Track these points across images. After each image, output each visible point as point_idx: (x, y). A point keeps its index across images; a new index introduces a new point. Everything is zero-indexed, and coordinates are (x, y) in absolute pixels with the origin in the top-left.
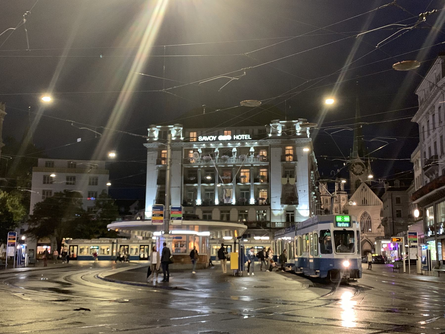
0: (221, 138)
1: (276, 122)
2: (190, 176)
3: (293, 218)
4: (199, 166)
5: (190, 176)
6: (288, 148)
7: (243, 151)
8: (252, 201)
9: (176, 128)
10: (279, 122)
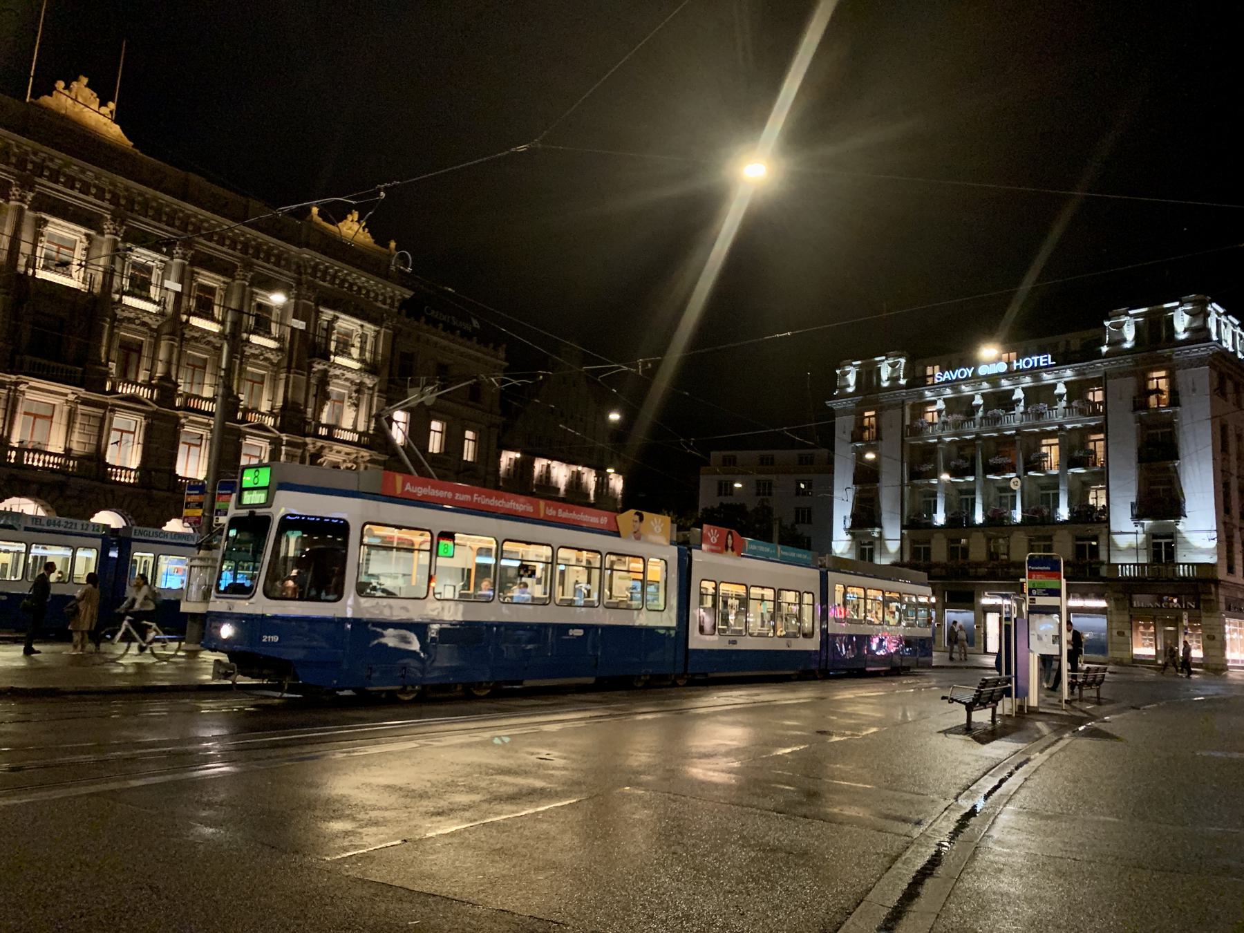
1: (1119, 315)
2: (926, 461)
3: (1171, 553)
4: (939, 438)
5: (920, 461)
6: (1156, 374)
7: (1040, 395)
8: (1063, 513)
9: (891, 361)
10: (1127, 314)
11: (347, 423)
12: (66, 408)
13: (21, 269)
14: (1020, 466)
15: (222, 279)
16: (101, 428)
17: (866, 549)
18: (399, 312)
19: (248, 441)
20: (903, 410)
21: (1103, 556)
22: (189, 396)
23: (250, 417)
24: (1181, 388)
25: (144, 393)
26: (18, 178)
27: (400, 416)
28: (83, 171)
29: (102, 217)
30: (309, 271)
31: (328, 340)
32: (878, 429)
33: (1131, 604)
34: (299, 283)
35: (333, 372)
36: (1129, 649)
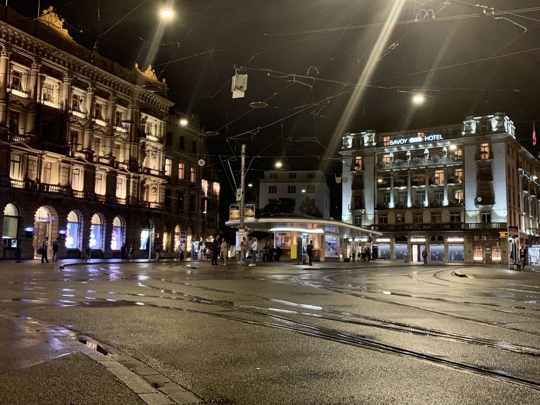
0: (412, 140)
1: (469, 119)
4: (391, 169)
6: (484, 145)
8: (446, 202)
9: (369, 134)
10: (473, 119)
14: (427, 182)
15: (105, 100)
16: (69, 172)
17: (357, 220)
20: (375, 156)
21: (462, 220)
24: (494, 150)
29: (63, 74)
30: (138, 95)
32: (363, 165)
33: (473, 240)
34: (133, 102)
35: (147, 143)
36: (472, 258)
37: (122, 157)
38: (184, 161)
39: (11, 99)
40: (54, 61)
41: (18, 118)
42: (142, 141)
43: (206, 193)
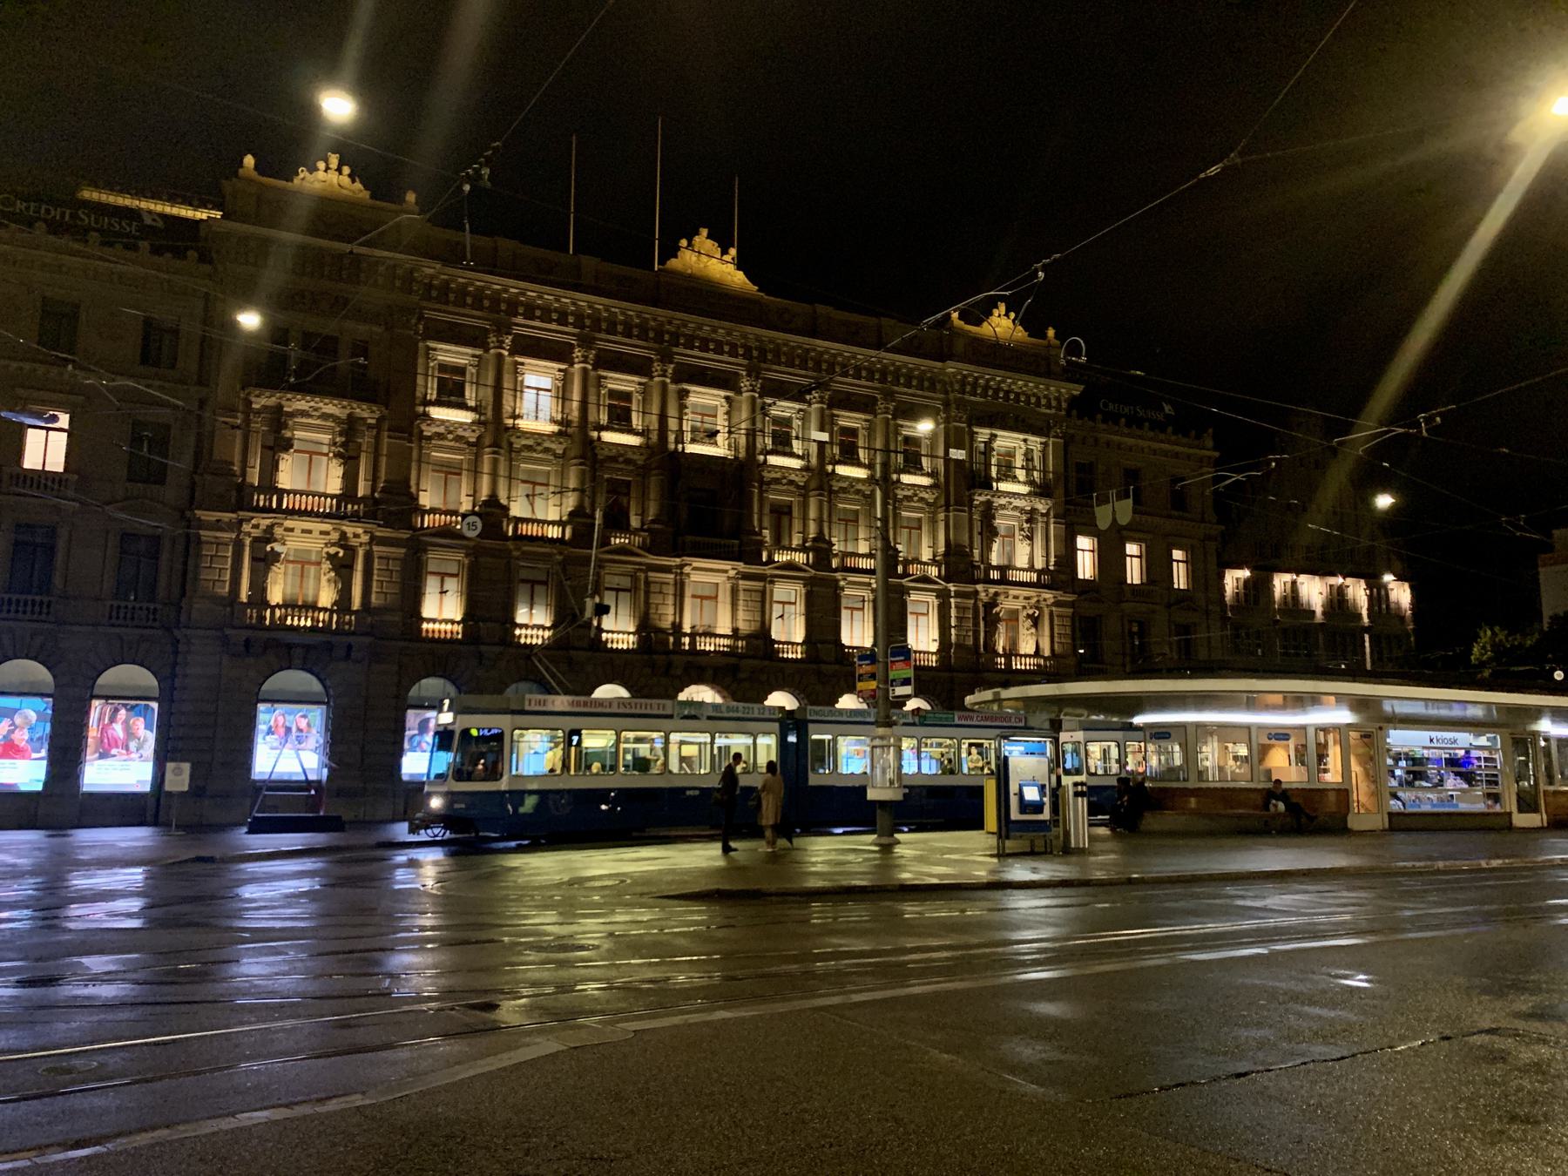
11: (1021, 560)
12: (729, 586)
13: (672, 446)
16: (763, 602)
18: (1069, 414)
19: (913, 597)
22: (846, 555)
23: (913, 569)
25: (800, 558)
26: (658, 352)
27: (1084, 542)
28: (714, 330)
30: (957, 387)
31: (988, 465)
34: (947, 404)
37: (926, 549)
38: (1142, 536)
39: (602, 454)
40: (707, 350)
41: (628, 494)
42: (980, 499)
43: (1364, 613)
